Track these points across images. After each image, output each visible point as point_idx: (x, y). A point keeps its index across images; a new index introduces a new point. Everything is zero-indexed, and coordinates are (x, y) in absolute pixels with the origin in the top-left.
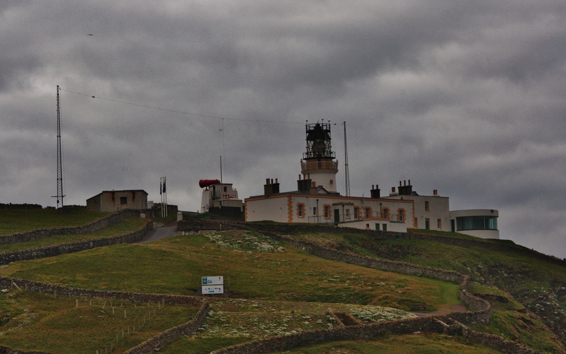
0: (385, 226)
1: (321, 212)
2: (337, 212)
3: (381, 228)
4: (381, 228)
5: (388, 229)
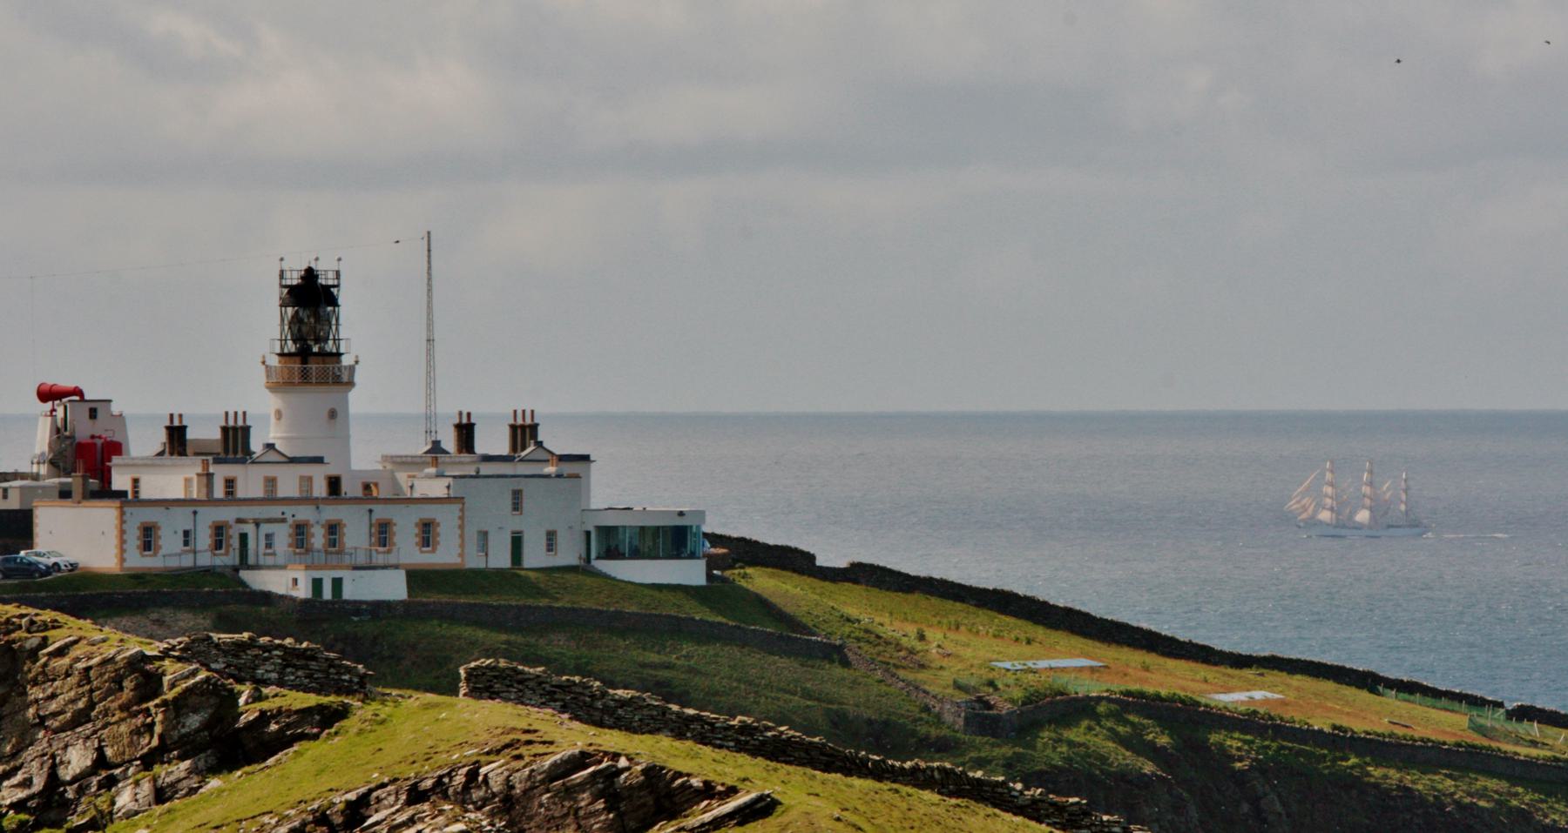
0: (337, 584)
1: (204, 539)
3: (327, 594)
4: (327, 594)
5: (348, 593)
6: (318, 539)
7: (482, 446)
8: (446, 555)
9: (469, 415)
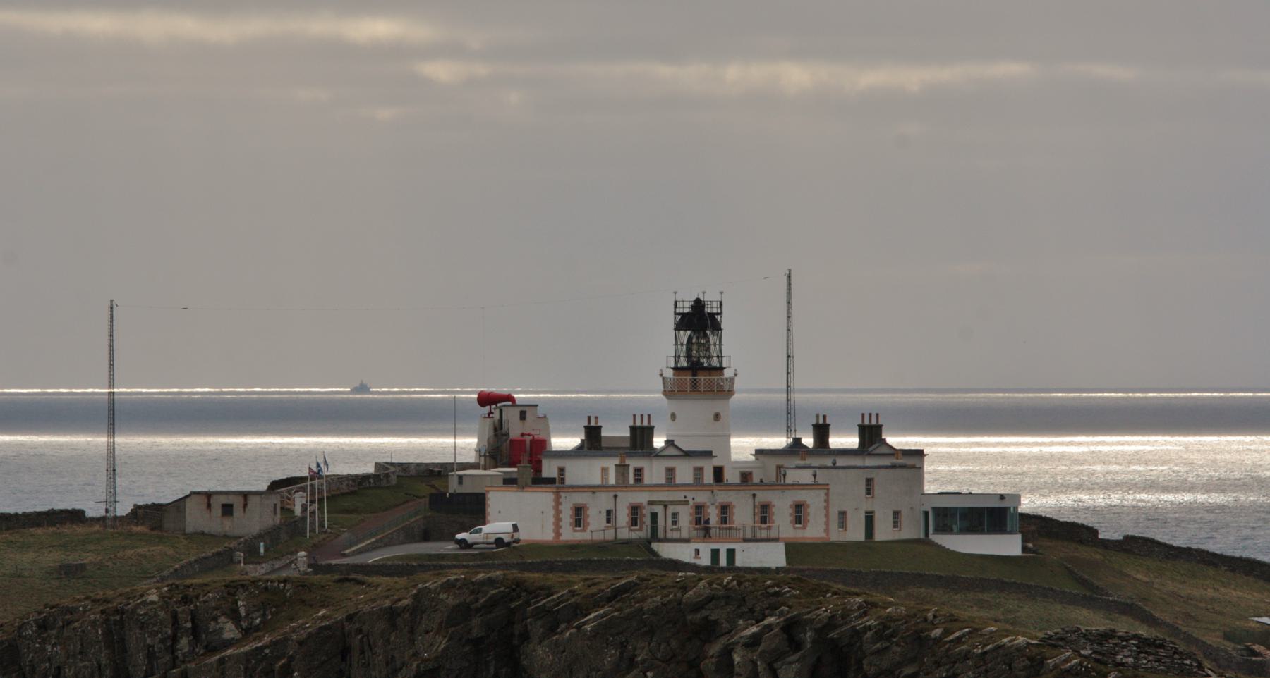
0: (731, 553)
1: (623, 517)
3: (723, 562)
4: (723, 562)
8: (814, 531)
9: (825, 417)
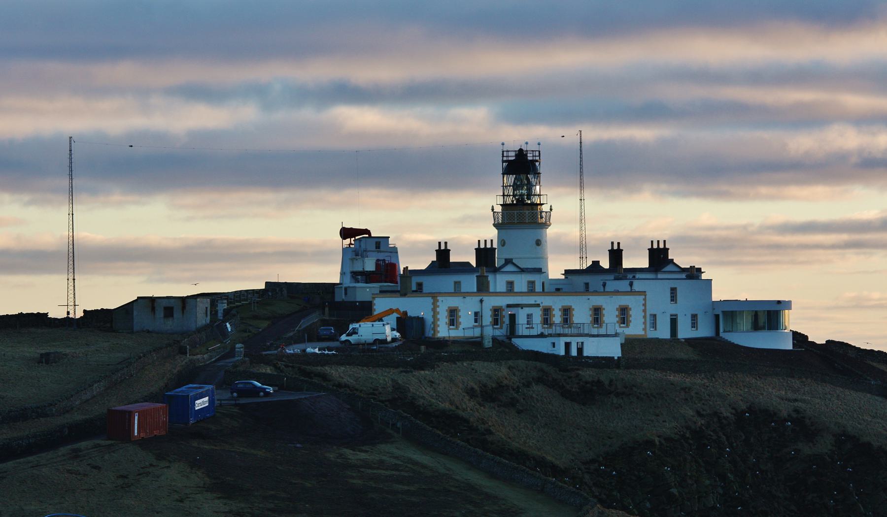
1: (487, 319)
2: (513, 317)
3: (574, 352)
4: (574, 352)
6: (557, 318)
7: (626, 264)
8: (636, 328)
9: (619, 244)
